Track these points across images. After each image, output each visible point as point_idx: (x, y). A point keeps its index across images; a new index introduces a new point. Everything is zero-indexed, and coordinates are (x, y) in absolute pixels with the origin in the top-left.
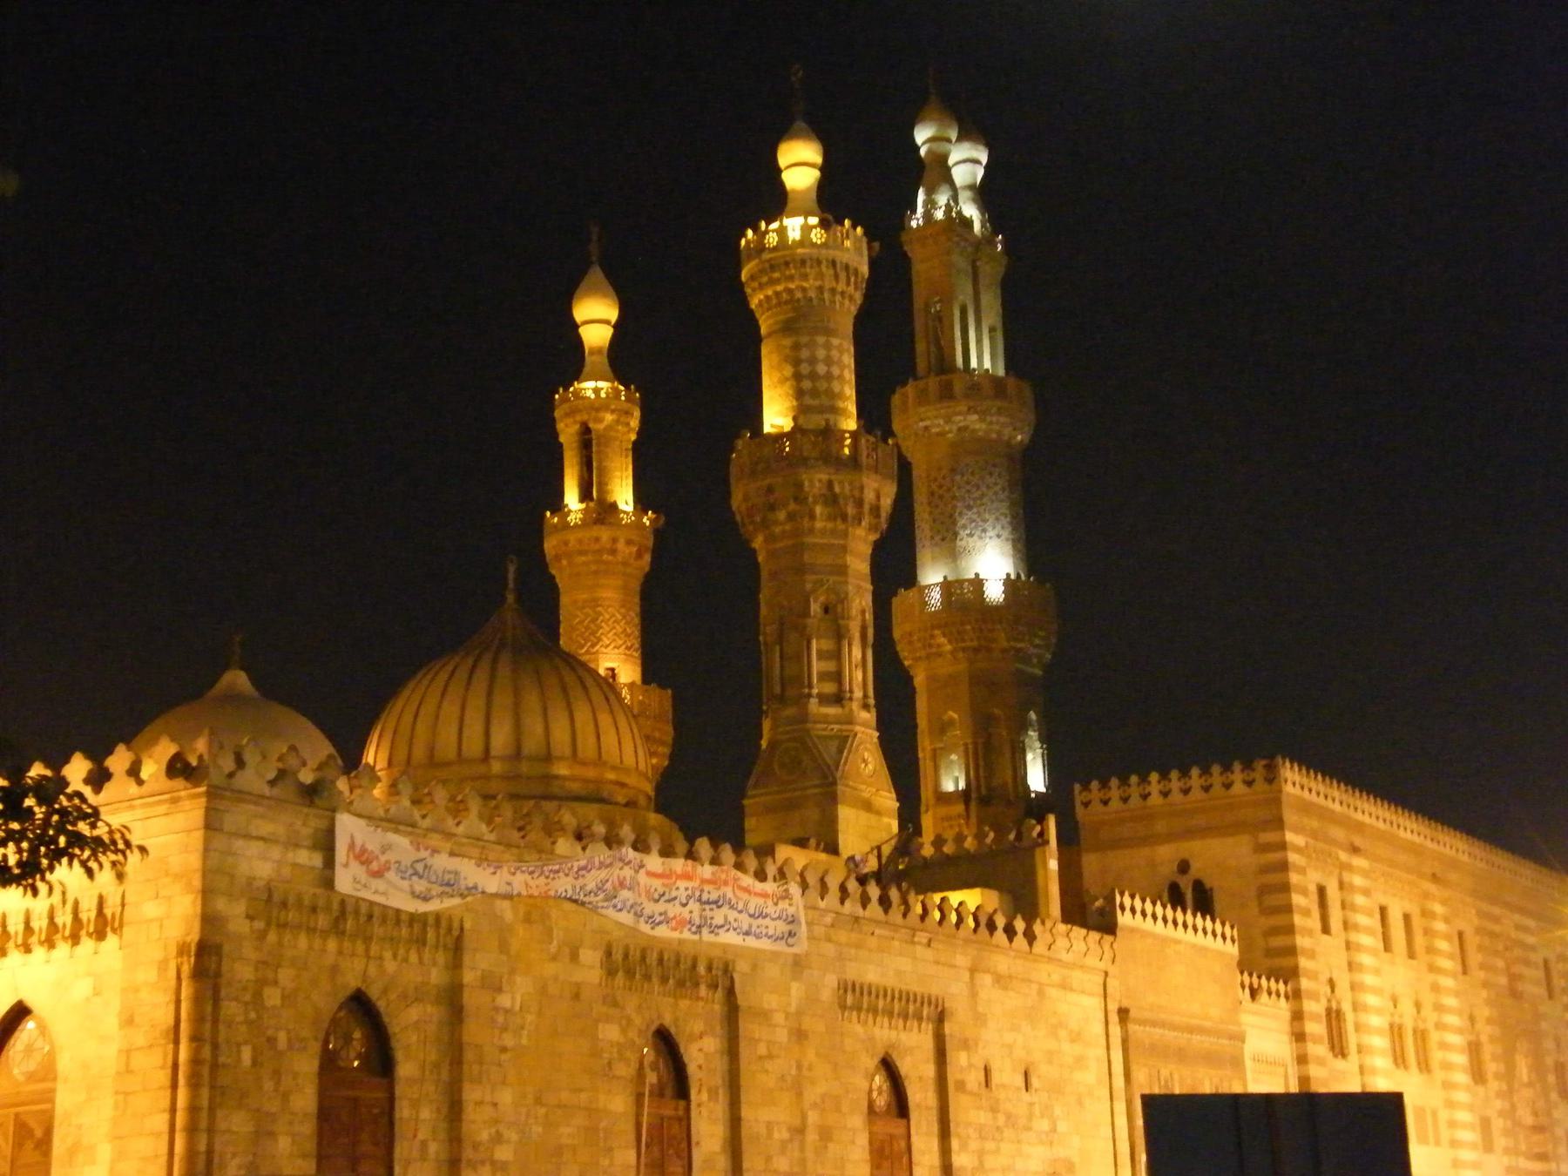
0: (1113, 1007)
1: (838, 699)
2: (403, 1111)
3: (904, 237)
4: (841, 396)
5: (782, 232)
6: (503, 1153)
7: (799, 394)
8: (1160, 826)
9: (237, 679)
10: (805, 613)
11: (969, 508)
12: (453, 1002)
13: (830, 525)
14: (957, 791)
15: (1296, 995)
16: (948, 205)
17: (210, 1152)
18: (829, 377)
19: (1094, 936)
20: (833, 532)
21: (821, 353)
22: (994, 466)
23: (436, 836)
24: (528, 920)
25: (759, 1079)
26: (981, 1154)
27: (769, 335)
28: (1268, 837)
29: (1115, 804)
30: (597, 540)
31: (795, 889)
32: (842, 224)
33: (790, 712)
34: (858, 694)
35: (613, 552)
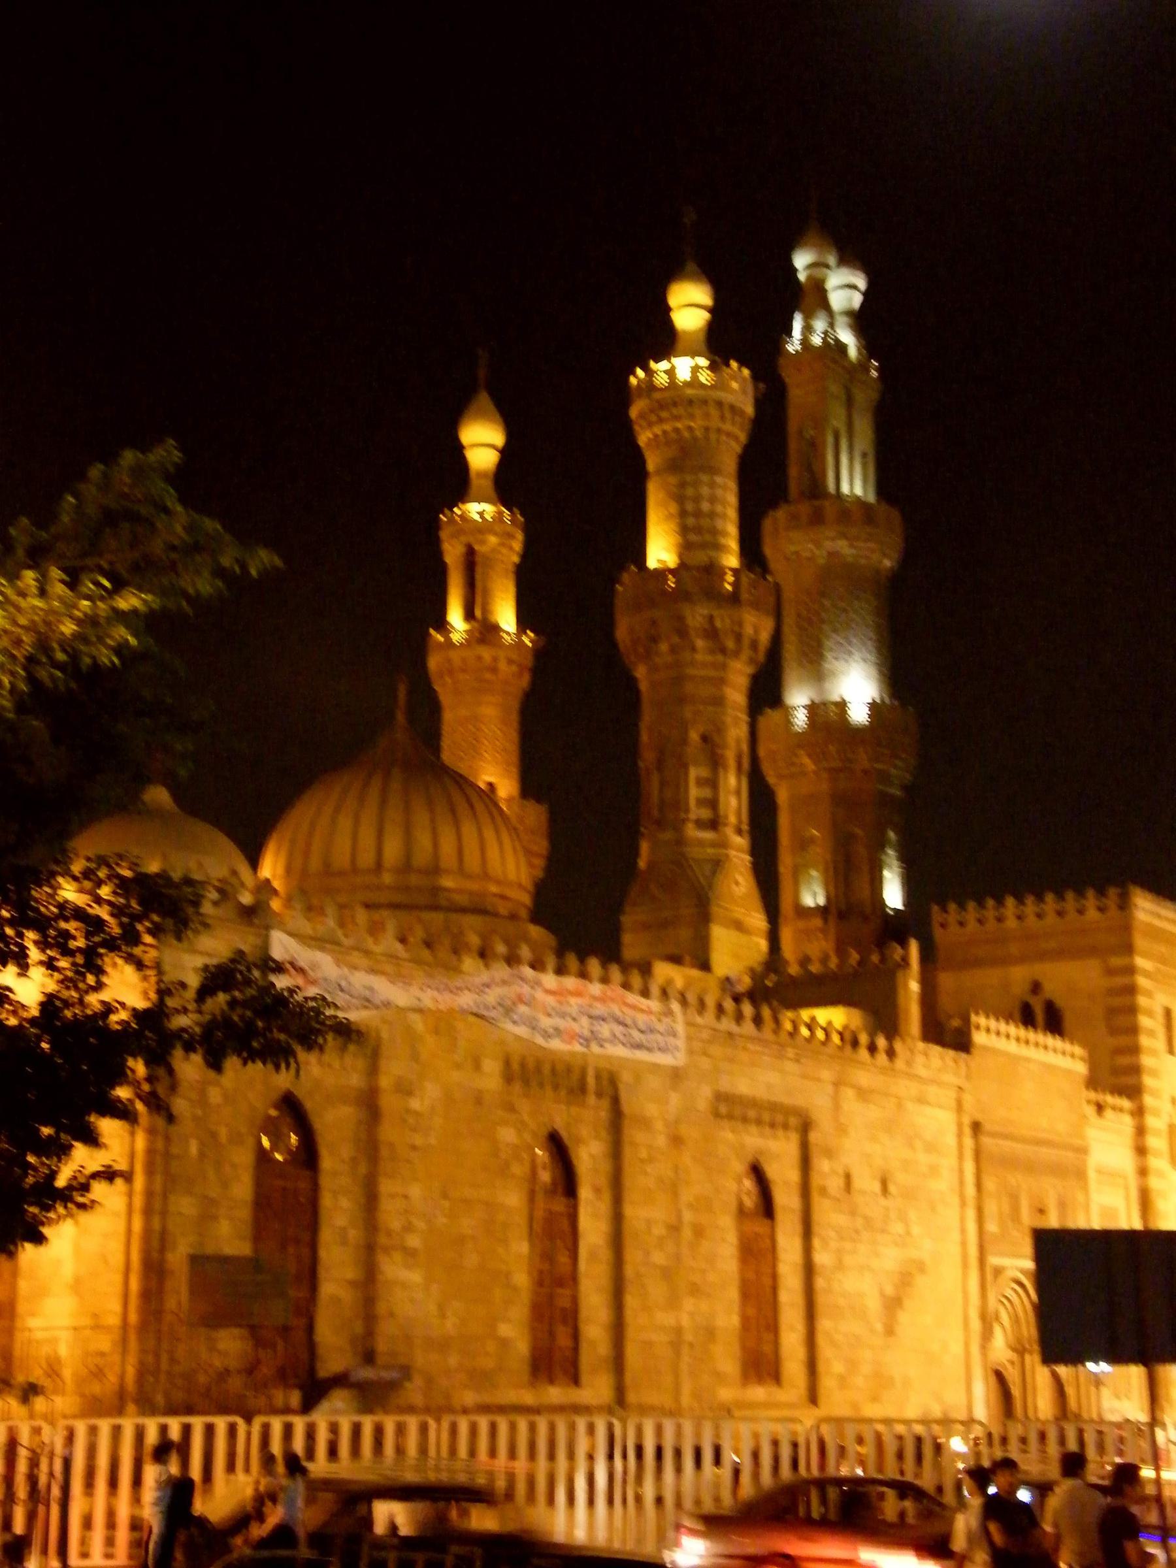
0: (967, 1121)
1: (714, 824)
2: (326, 1201)
3: (782, 361)
4: (724, 534)
5: (671, 373)
6: (413, 1241)
7: (684, 530)
8: (1014, 949)
9: (159, 795)
10: (684, 741)
12: (370, 1104)
13: (709, 658)
14: (818, 907)
15: (1139, 1112)
16: (826, 333)
17: (164, 1233)
18: (712, 515)
19: (950, 1053)
20: (714, 666)
21: (705, 491)
23: (356, 953)
24: (436, 1031)
25: (637, 1181)
26: (839, 1252)
27: (658, 472)
28: (1116, 961)
29: (972, 925)
30: (479, 658)
31: (675, 1006)
32: (728, 365)
33: (668, 835)
34: (733, 819)
35: (494, 670)
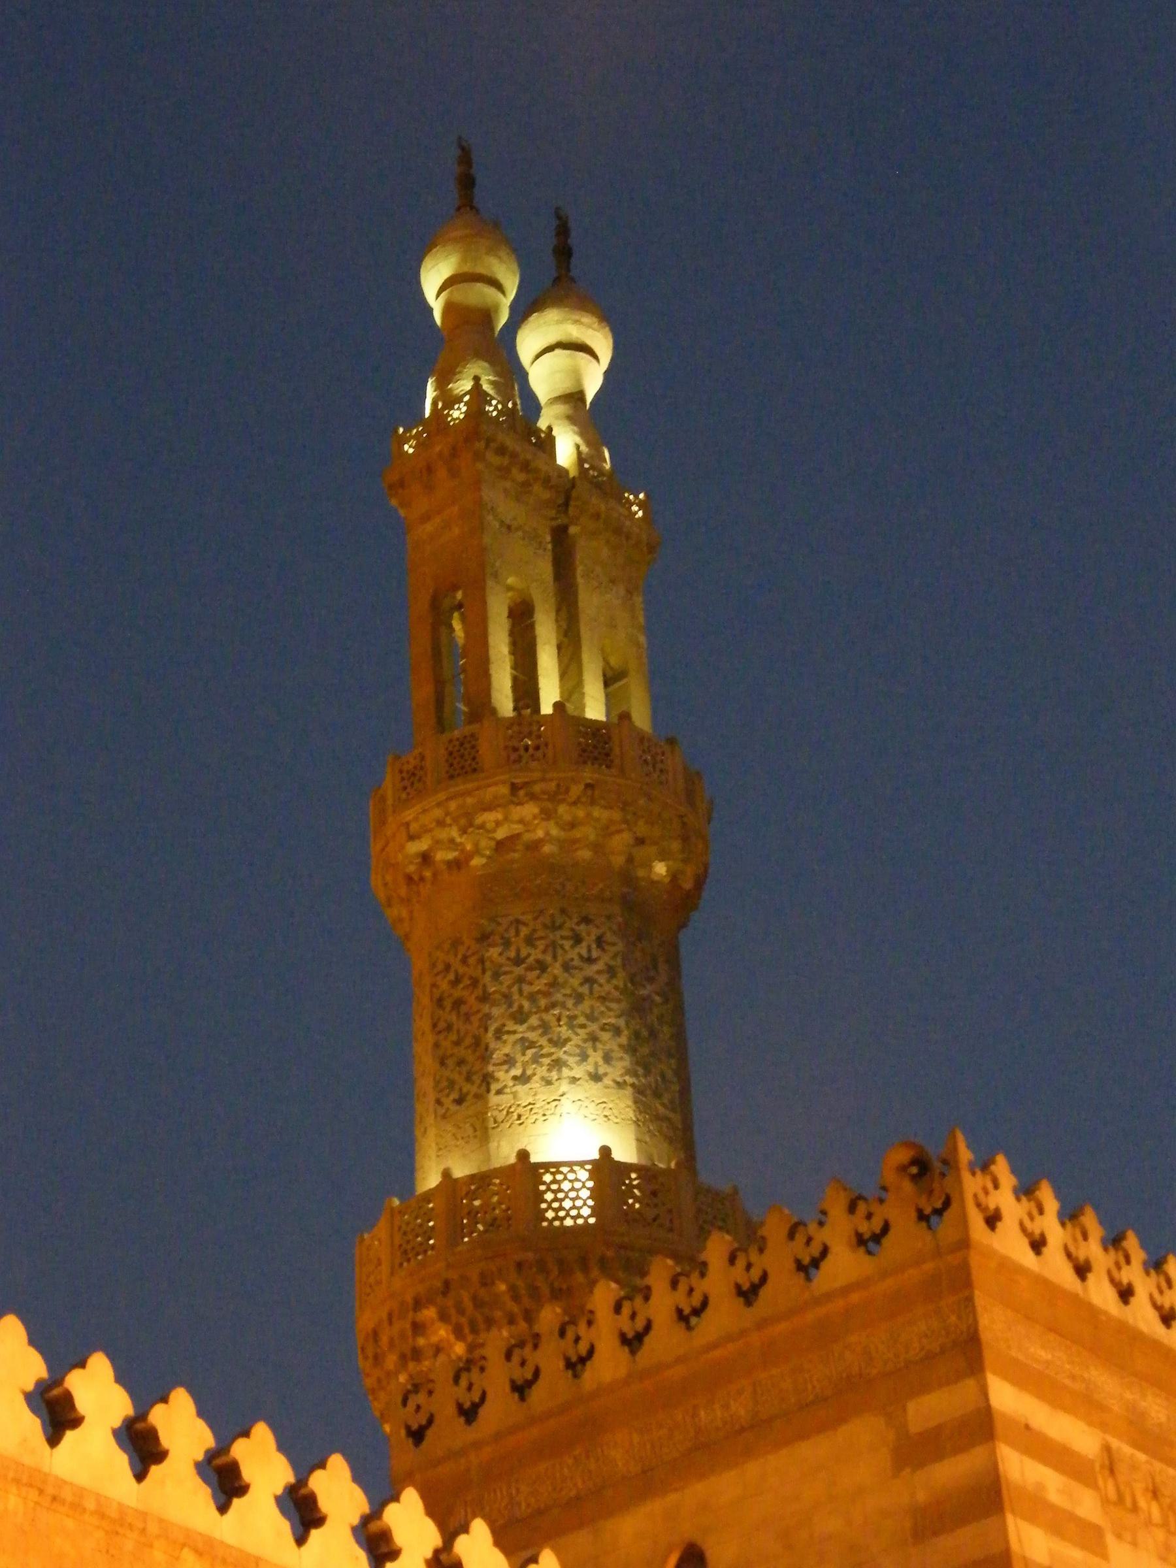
8: (620, 1451)
11: (520, 1017)
22: (586, 920)
